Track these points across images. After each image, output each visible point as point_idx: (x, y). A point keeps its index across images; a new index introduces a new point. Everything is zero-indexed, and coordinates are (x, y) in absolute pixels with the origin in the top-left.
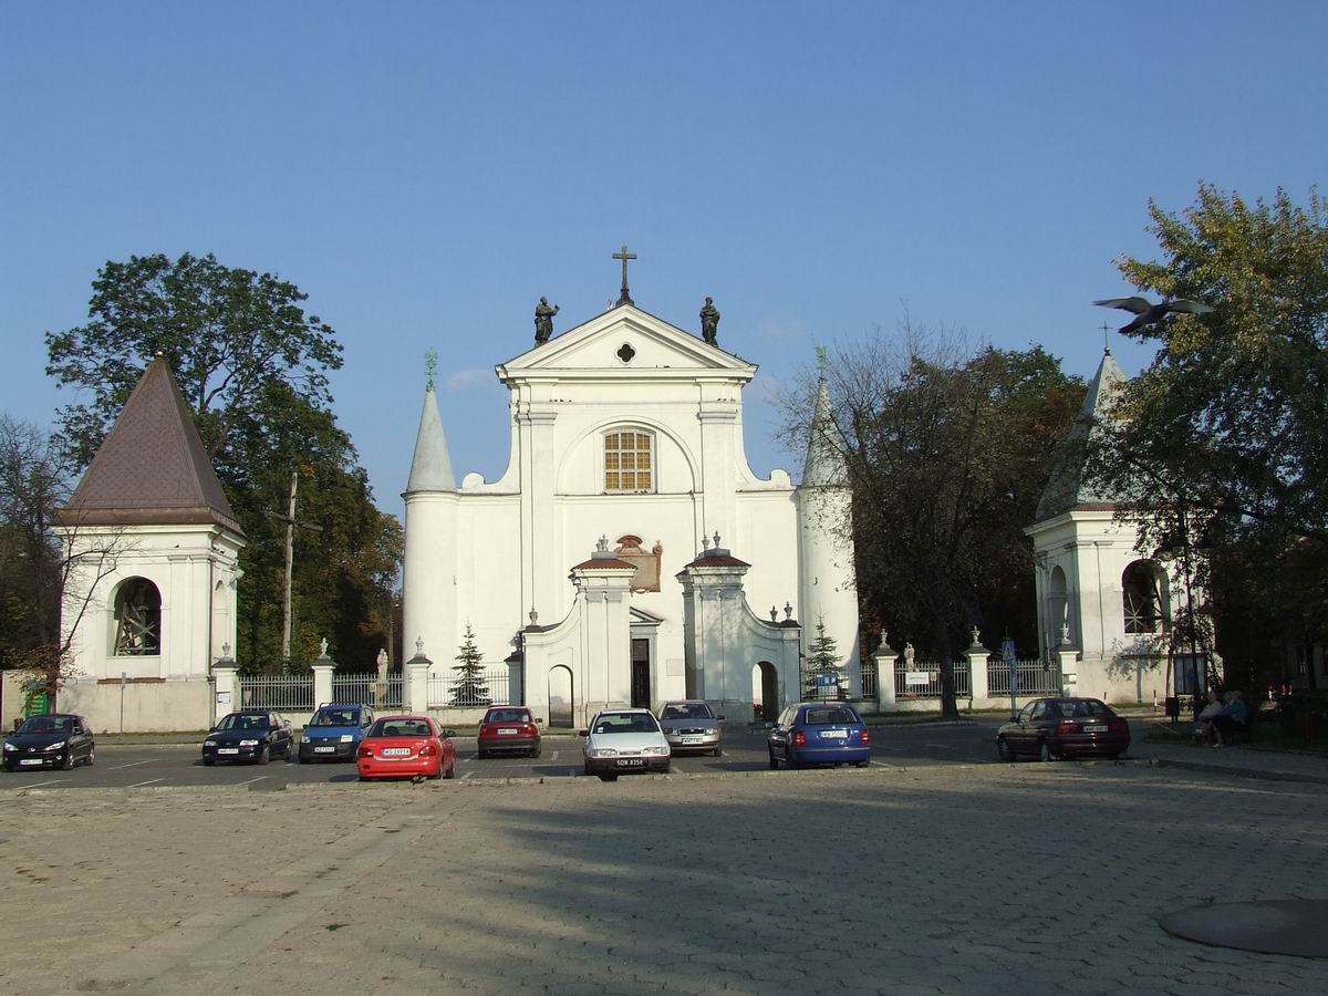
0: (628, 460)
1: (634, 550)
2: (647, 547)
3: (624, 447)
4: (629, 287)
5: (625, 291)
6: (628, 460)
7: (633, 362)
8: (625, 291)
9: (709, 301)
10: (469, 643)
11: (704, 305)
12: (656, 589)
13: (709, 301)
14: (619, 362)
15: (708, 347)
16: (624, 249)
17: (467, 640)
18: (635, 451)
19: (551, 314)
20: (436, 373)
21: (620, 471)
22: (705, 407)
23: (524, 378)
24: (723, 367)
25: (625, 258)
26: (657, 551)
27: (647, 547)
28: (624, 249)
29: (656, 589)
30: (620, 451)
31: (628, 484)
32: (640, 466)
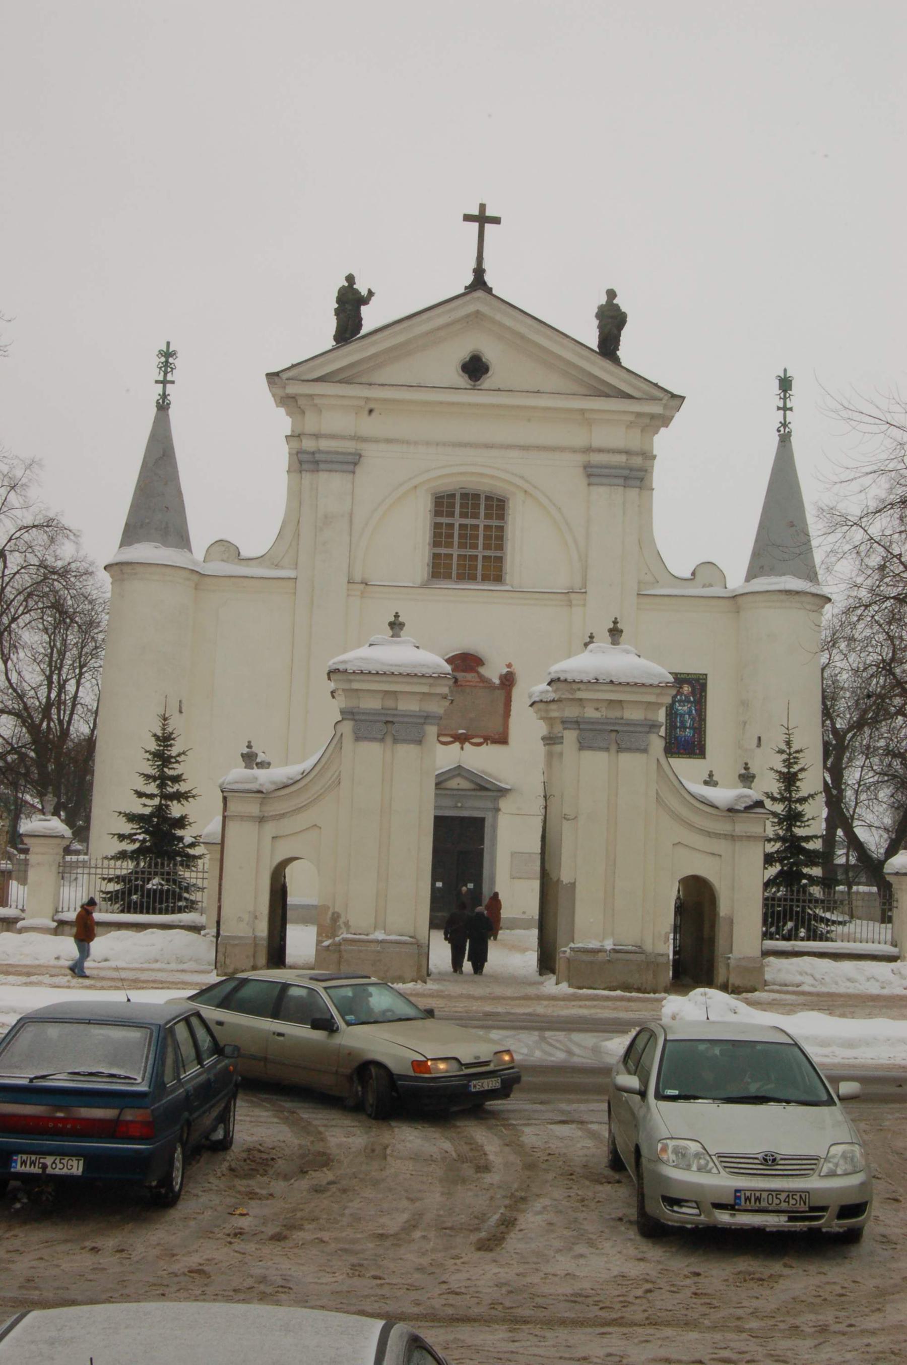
0: (468, 536)
1: (470, 676)
2: (493, 672)
3: (463, 515)
4: (486, 265)
5: (479, 272)
6: (468, 536)
7: (487, 382)
8: (479, 272)
9: (611, 294)
10: (160, 811)
11: (603, 300)
12: (502, 739)
13: (611, 294)
14: (462, 380)
15: (607, 364)
16: (482, 207)
17: (156, 801)
18: (481, 522)
19: (365, 301)
20: (173, 382)
21: (455, 552)
22: (596, 458)
23: (311, 396)
24: (629, 397)
25: (482, 219)
26: (508, 681)
27: (493, 672)
28: (482, 207)
29: (502, 739)
30: (457, 521)
31: (467, 574)
32: (487, 547)
